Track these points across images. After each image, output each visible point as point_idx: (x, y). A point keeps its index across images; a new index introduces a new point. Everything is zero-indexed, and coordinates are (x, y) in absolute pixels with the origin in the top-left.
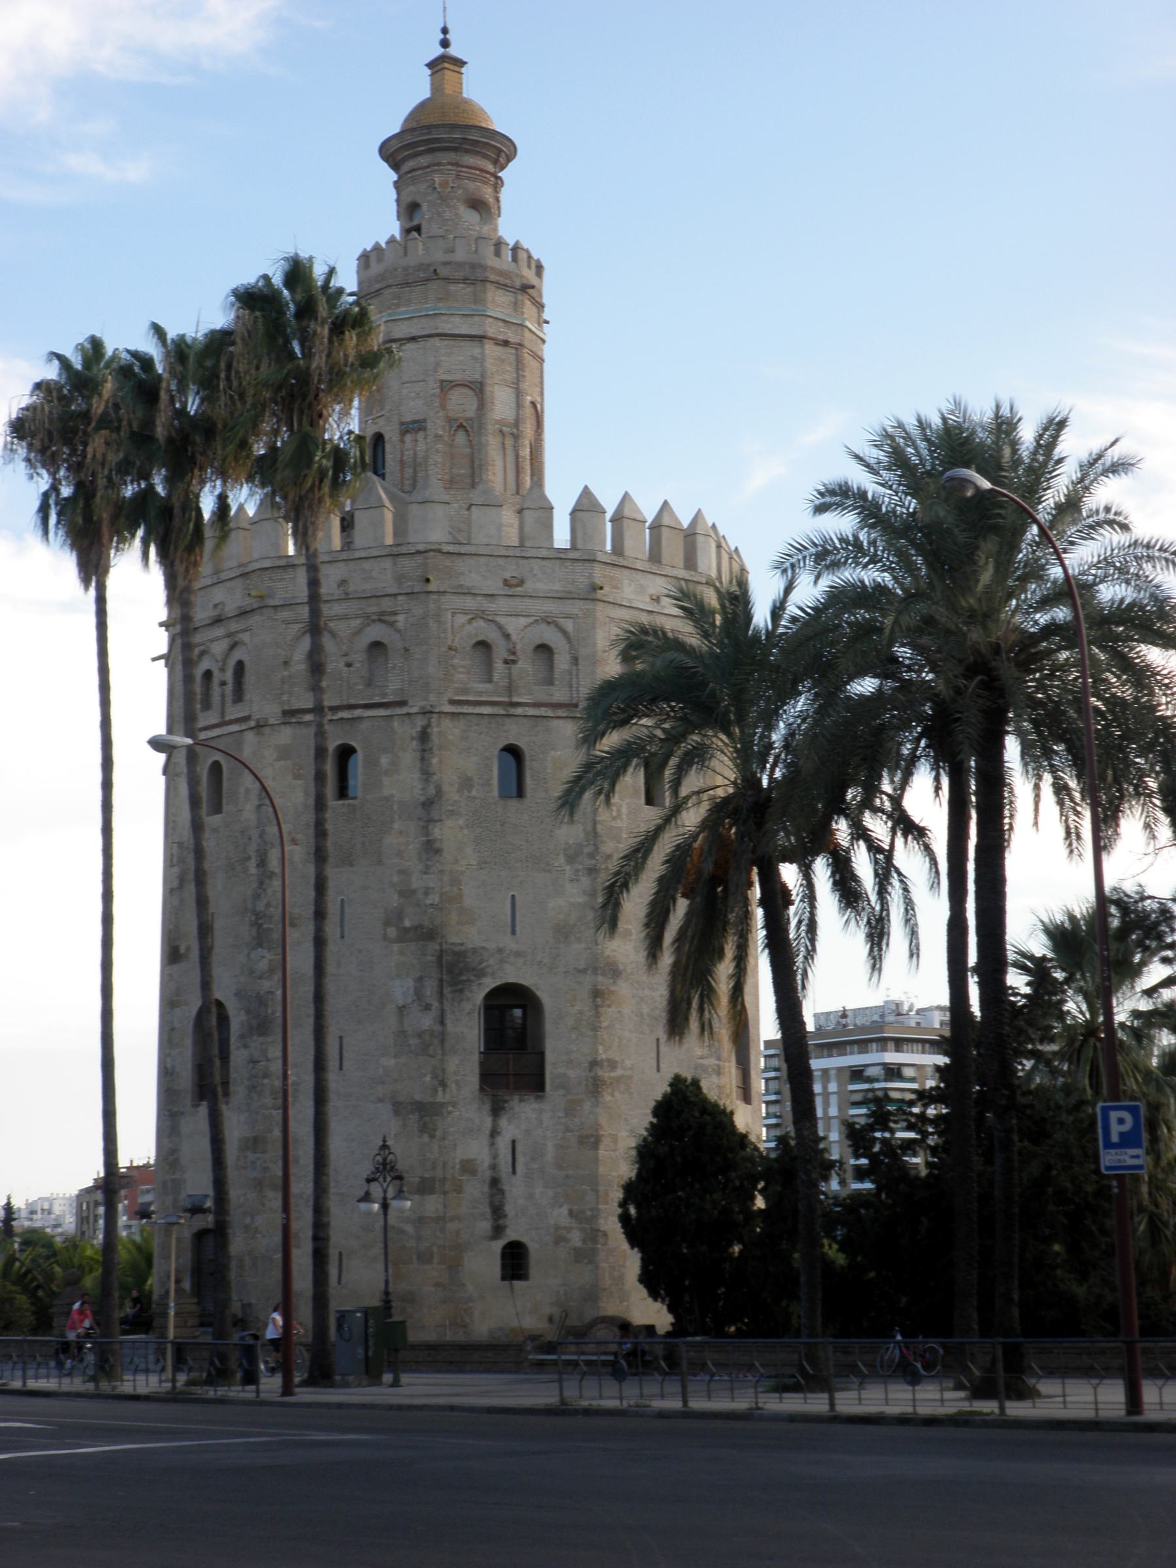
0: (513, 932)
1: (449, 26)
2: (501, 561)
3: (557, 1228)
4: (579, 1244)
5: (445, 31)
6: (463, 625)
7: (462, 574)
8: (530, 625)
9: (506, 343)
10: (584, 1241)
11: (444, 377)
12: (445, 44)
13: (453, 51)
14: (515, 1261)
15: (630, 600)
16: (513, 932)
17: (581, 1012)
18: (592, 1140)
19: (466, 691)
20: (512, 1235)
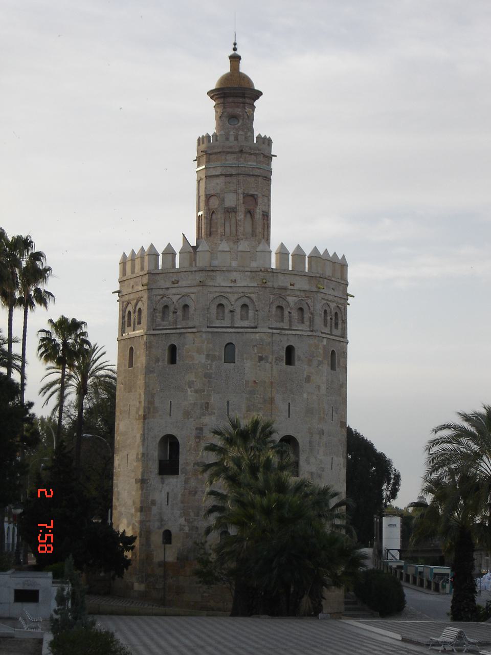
0: (170, 415)
1: (236, 42)
2: (171, 274)
3: (180, 525)
4: (187, 531)
5: (235, 44)
6: (159, 301)
7: (158, 281)
8: (180, 299)
9: (231, 175)
10: (189, 530)
11: (207, 193)
12: (235, 49)
13: (238, 52)
14: (167, 537)
15: (219, 284)
16: (170, 415)
17: (191, 444)
18: (193, 492)
19: (159, 325)
20: (166, 528)
